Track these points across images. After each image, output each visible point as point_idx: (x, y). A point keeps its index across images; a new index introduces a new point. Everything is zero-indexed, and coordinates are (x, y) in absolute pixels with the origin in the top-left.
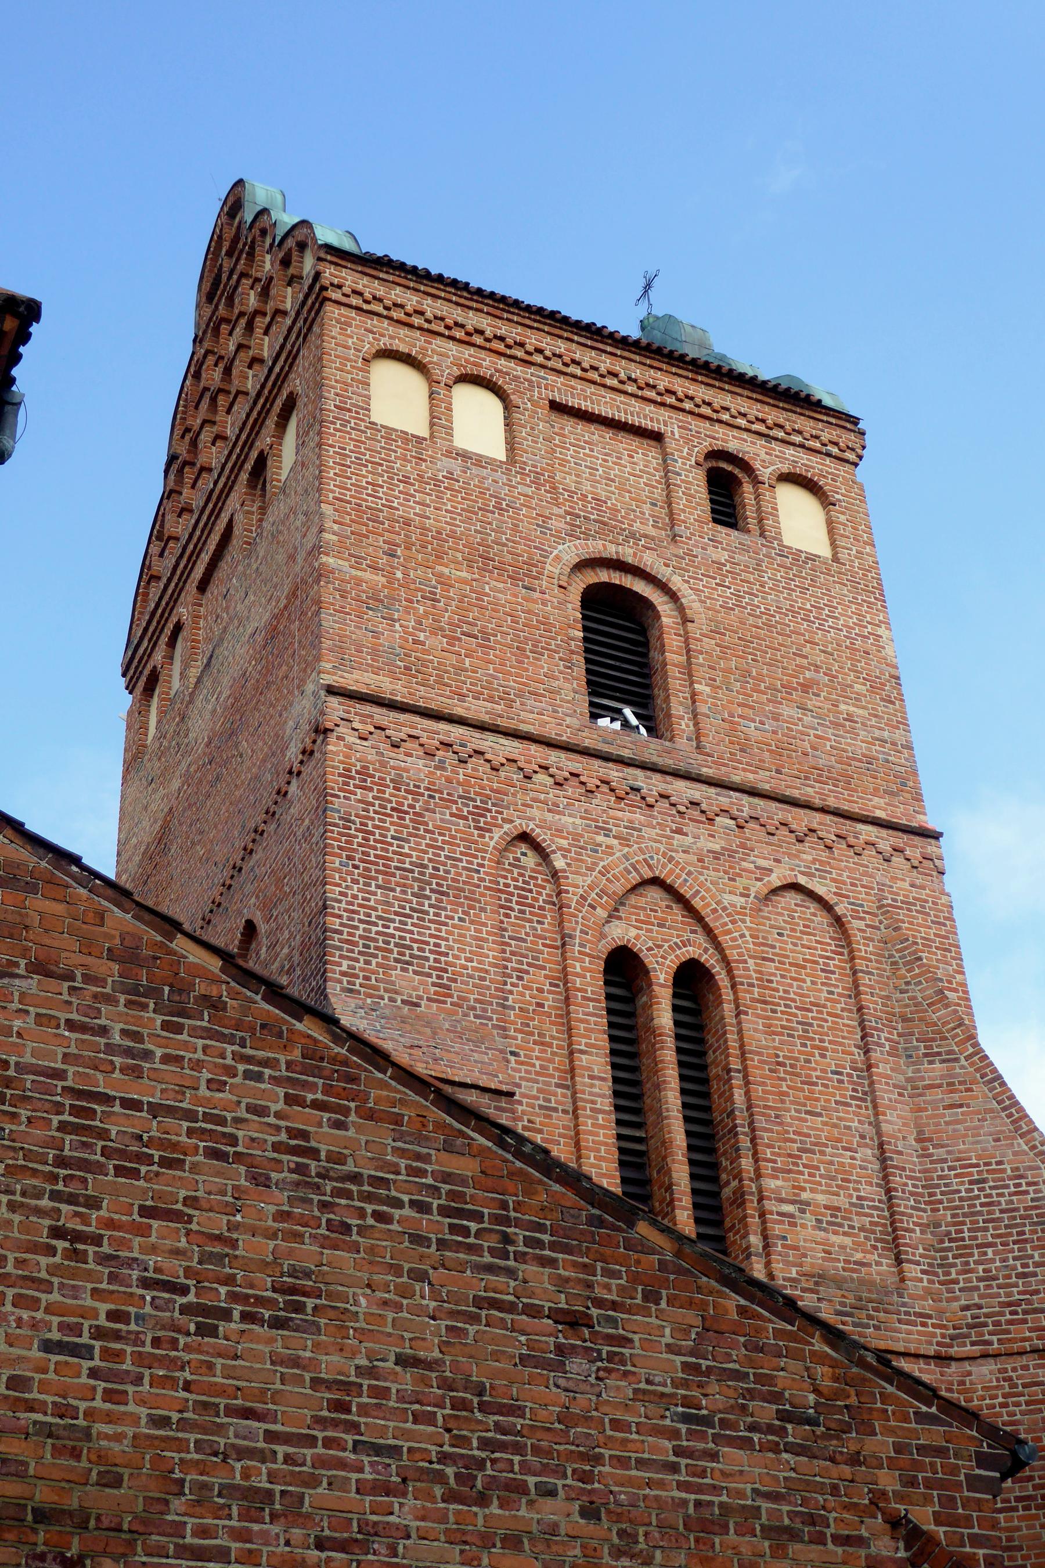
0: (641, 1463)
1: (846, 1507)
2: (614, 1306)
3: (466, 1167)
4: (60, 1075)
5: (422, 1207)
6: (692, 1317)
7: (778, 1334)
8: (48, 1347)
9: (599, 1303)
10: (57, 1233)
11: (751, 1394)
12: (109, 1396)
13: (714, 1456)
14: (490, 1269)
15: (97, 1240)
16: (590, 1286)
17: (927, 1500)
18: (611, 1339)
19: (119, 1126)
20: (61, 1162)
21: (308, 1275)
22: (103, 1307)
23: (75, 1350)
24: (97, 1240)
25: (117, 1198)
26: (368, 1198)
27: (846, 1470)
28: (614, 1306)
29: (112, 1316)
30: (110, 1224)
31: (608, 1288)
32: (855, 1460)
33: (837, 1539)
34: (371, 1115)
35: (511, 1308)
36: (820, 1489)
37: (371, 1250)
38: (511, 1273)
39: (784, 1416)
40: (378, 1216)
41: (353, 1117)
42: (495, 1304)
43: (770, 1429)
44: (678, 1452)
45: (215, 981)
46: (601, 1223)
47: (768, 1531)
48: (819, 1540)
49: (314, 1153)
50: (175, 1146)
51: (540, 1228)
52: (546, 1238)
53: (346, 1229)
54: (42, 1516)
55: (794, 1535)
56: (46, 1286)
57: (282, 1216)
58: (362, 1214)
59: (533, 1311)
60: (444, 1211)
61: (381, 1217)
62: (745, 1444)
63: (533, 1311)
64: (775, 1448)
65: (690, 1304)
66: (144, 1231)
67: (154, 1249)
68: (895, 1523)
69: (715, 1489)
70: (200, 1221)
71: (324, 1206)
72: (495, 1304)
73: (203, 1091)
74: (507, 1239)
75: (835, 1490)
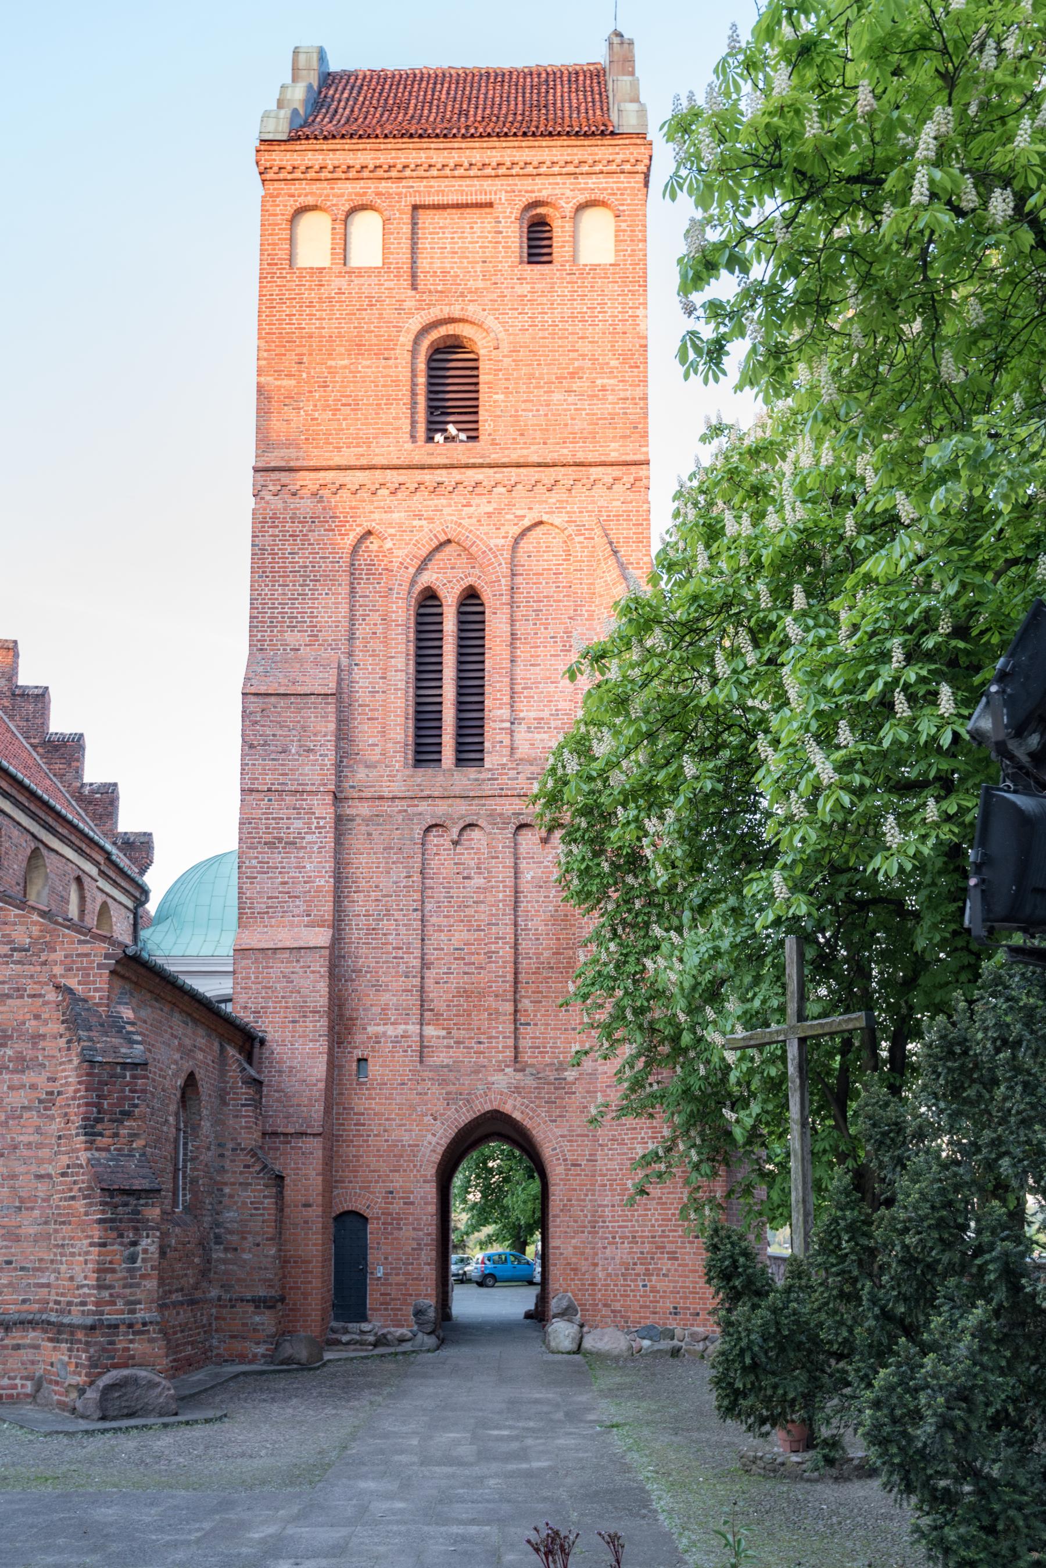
17: (75, 976)
27: (38, 968)
32: (44, 963)
33: (29, 996)
48: (22, 997)
68: (57, 987)
75: (32, 977)
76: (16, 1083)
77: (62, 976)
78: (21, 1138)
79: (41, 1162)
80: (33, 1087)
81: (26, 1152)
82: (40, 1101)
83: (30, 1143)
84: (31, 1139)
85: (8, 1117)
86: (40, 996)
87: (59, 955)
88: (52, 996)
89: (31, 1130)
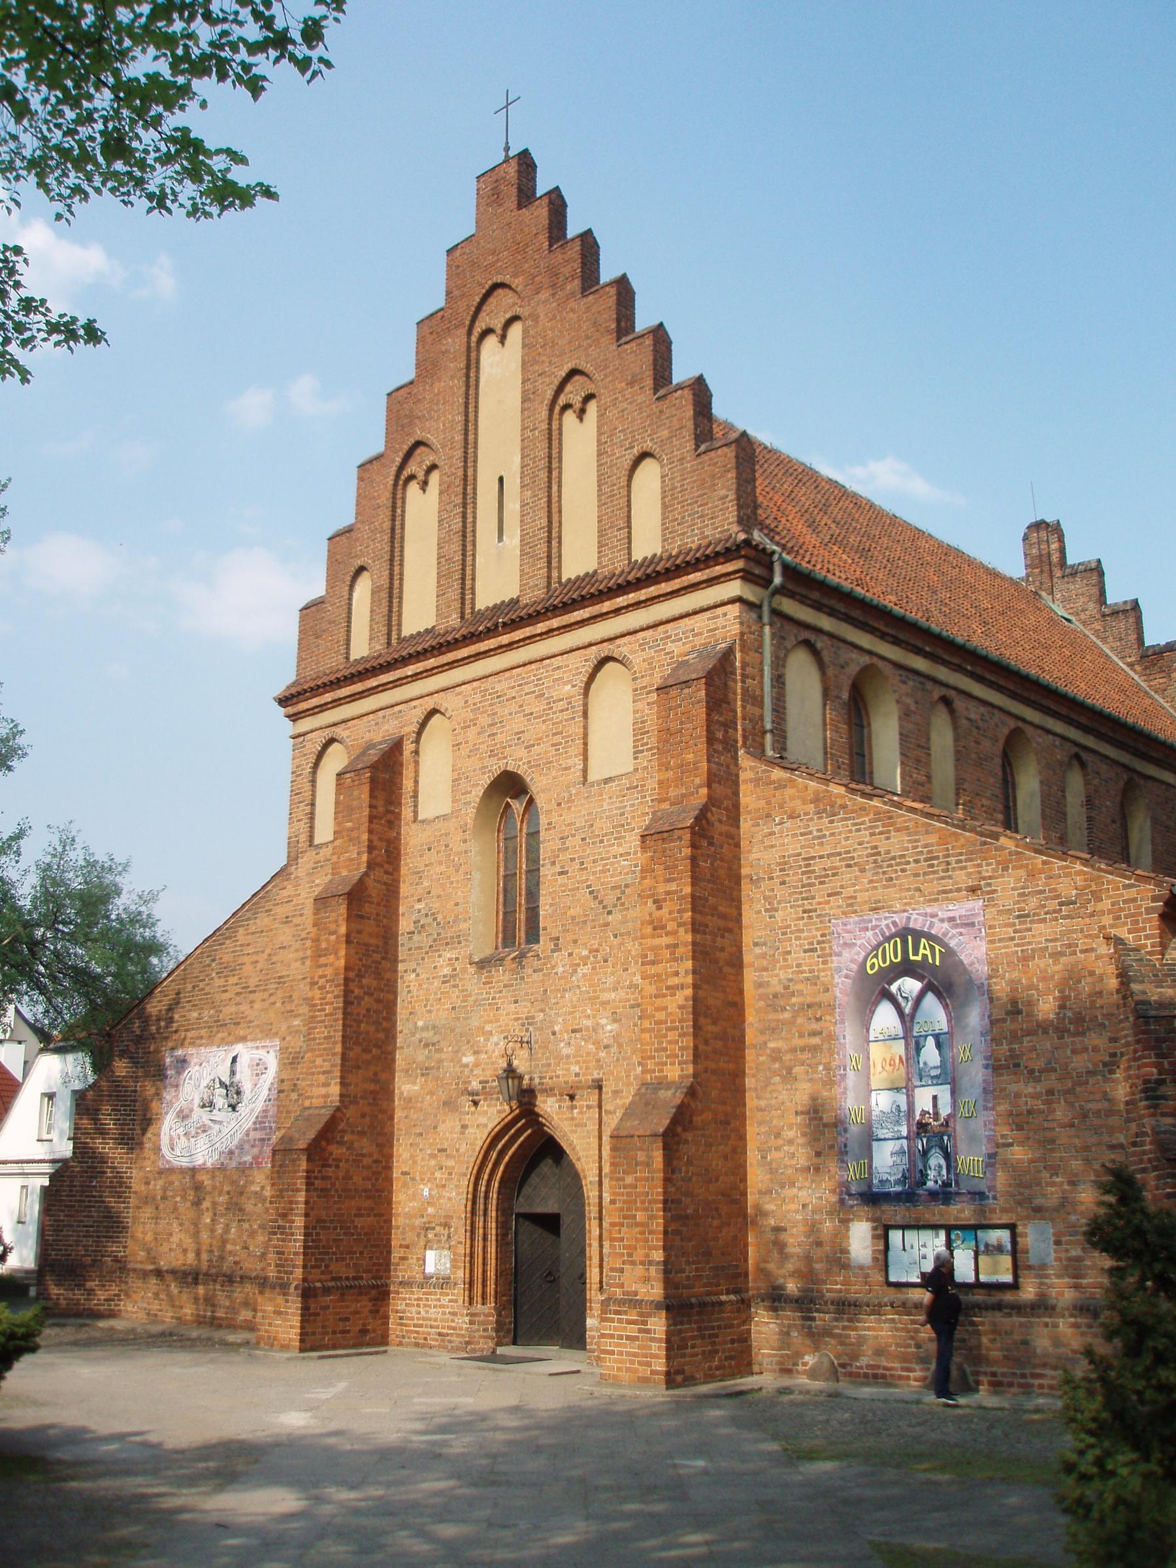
0: (1000, 940)
1: (1086, 937)
2: (990, 878)
3: (933, 839)
4: (800, 854)
5: (917, 861)
6: (1022, 873)
7: (1060, 868)
8: (805, 951)
9: (984, 878)
10: (804, 912)
11: (1046, 899)
12: (825, 963)
13: (1030, 930)
14: (942, 878)
15: (815, 910)
16: (980, 872)
18: (989, 893)
19: (817, 866)
20: (803, 887)
21: (879, 901)
22: (819, 933)
23: (812, 950)
24: (815, 910)
25: (820, 893)
26: (898, 864)
28: (990, 878)
29: (823, 935)
30: (819, 903)
31: (987, 871)
32: (1092, 915)
33: (1082, 952)
34: (898, 830)
35: (951, 891)
36: (1075, 931)
37: (900, 885)
38: (950, 877)
39: (1061, 904)
40: (903, 871)
41: (893, 833)
42: (945, 892)
43: (1055, 911)
44: (1015, 931)
45: (843, 797)
46: (985, 843)
47: (1052, 955)
49: (879, 854)
50: (835, 868)
51: (961, 854)
52: (963, 858)
53: (891, 879)
54: (809, 1006)
55: (1062, 954)
56: (802, 931)
57: (871, 882)
58: (896, 871)
59: (959, 890)
60: (926, 860)
61: (903, 871)
62: (1044, 921)
63: (959, 890)
64: (1056, 919)
65: (1021, 867)
66: (828, 902)
67: (832, 908)
69: (1029, 943)
70: (847, 892)
71: (884, 873)
72: (945, 892)
73: (843, 843)
74: (948, 863)
75: (1082, 931)
76: (1079, 1046)
77: (1112, 926)
78: (1090, 1105)
79: (1111, 1131)
80: (1096, 1049)
81: (1096, 1121)
82: (1105, 1064)
83: (1098, 1111)
84: (1098, 1106)
85: (1074, 1084)
86: (1092, 950)
87: (1106, 904)
88: (1105, 950)
89: (1098, 1096)
